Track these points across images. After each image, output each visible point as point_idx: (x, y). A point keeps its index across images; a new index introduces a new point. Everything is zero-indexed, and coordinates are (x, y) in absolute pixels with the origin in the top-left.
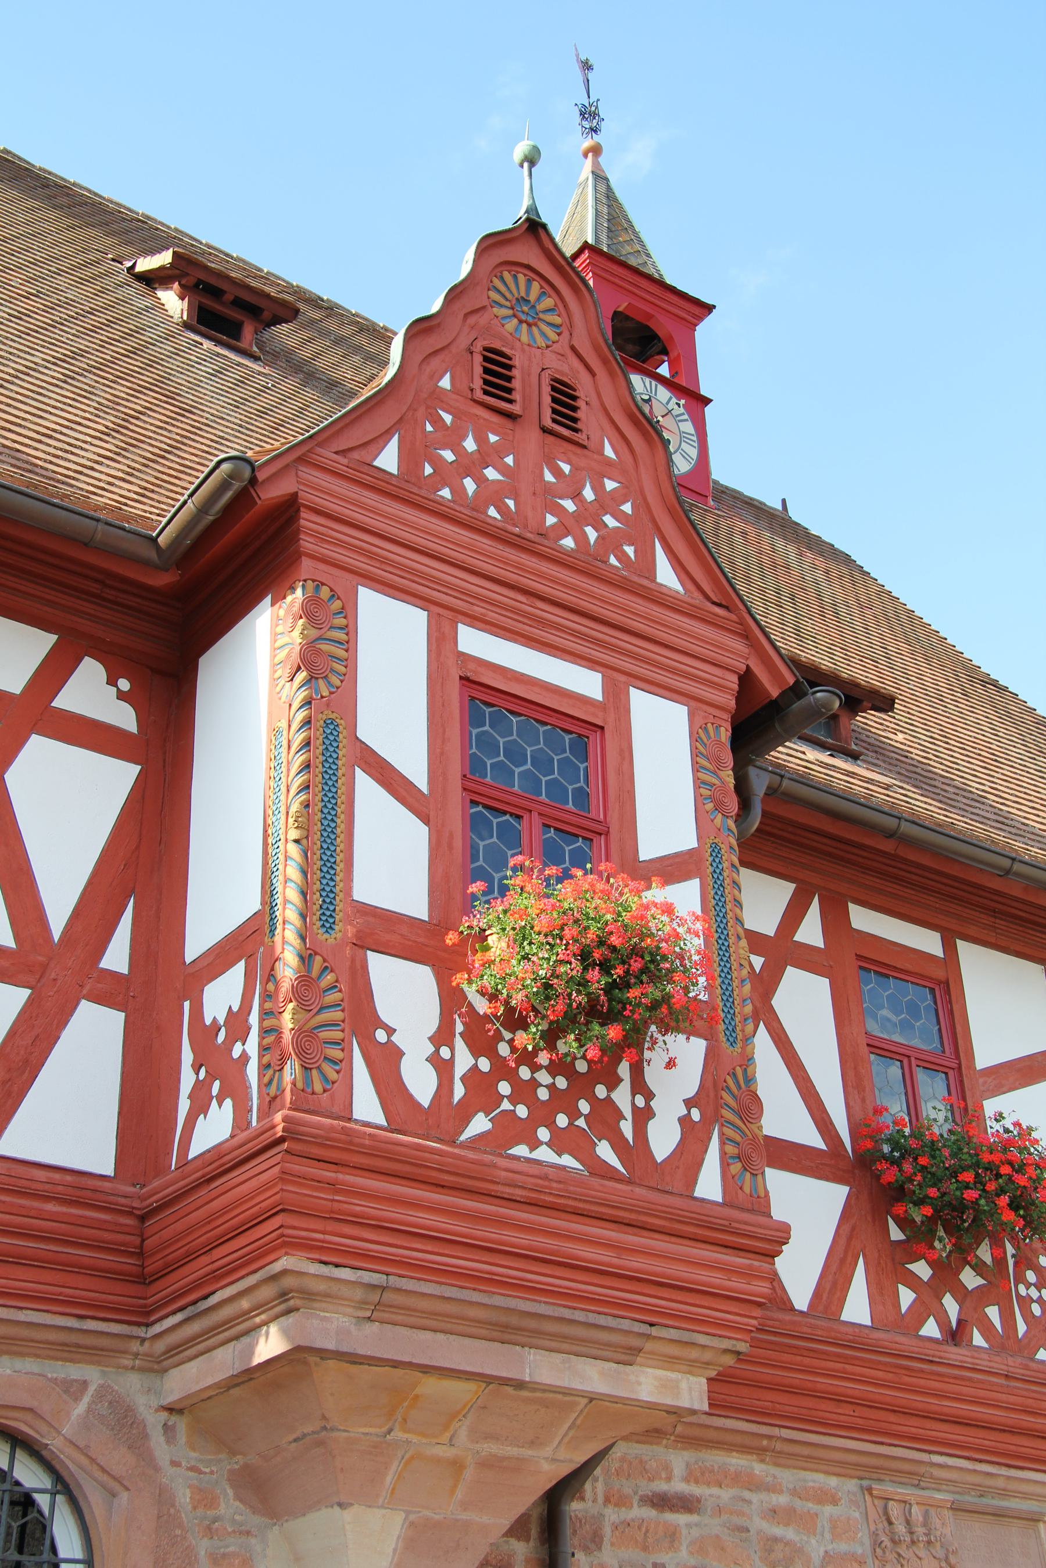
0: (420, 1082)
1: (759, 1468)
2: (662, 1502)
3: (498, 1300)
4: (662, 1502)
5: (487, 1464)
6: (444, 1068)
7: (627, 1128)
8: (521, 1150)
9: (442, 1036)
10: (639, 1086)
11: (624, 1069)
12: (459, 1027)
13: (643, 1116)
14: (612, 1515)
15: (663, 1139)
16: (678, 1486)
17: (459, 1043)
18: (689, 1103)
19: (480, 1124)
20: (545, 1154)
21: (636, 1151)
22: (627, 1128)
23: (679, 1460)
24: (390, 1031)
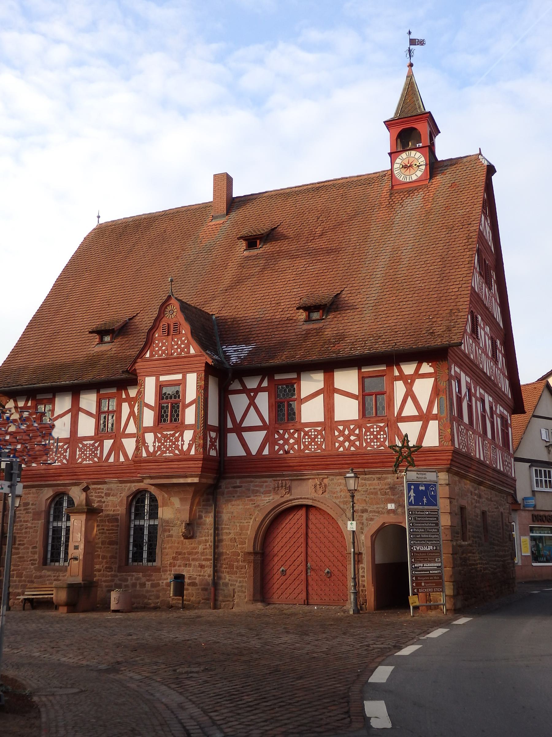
0: (151, 449)
1: (252, 479)
2: (235, 487)
4: (235, 487)
6: (154, 446)
8: (164, 455)
9: (154, 442)
10: (183, 440)
11: (180, 439)
13: (182, 445)
14: (226, 490)
15: (185, 448)
16: (238, 484)
19: (159, 452)
20: (168, 454)
21: (181, 451)
22: (180, 447)
23: (238, 481)
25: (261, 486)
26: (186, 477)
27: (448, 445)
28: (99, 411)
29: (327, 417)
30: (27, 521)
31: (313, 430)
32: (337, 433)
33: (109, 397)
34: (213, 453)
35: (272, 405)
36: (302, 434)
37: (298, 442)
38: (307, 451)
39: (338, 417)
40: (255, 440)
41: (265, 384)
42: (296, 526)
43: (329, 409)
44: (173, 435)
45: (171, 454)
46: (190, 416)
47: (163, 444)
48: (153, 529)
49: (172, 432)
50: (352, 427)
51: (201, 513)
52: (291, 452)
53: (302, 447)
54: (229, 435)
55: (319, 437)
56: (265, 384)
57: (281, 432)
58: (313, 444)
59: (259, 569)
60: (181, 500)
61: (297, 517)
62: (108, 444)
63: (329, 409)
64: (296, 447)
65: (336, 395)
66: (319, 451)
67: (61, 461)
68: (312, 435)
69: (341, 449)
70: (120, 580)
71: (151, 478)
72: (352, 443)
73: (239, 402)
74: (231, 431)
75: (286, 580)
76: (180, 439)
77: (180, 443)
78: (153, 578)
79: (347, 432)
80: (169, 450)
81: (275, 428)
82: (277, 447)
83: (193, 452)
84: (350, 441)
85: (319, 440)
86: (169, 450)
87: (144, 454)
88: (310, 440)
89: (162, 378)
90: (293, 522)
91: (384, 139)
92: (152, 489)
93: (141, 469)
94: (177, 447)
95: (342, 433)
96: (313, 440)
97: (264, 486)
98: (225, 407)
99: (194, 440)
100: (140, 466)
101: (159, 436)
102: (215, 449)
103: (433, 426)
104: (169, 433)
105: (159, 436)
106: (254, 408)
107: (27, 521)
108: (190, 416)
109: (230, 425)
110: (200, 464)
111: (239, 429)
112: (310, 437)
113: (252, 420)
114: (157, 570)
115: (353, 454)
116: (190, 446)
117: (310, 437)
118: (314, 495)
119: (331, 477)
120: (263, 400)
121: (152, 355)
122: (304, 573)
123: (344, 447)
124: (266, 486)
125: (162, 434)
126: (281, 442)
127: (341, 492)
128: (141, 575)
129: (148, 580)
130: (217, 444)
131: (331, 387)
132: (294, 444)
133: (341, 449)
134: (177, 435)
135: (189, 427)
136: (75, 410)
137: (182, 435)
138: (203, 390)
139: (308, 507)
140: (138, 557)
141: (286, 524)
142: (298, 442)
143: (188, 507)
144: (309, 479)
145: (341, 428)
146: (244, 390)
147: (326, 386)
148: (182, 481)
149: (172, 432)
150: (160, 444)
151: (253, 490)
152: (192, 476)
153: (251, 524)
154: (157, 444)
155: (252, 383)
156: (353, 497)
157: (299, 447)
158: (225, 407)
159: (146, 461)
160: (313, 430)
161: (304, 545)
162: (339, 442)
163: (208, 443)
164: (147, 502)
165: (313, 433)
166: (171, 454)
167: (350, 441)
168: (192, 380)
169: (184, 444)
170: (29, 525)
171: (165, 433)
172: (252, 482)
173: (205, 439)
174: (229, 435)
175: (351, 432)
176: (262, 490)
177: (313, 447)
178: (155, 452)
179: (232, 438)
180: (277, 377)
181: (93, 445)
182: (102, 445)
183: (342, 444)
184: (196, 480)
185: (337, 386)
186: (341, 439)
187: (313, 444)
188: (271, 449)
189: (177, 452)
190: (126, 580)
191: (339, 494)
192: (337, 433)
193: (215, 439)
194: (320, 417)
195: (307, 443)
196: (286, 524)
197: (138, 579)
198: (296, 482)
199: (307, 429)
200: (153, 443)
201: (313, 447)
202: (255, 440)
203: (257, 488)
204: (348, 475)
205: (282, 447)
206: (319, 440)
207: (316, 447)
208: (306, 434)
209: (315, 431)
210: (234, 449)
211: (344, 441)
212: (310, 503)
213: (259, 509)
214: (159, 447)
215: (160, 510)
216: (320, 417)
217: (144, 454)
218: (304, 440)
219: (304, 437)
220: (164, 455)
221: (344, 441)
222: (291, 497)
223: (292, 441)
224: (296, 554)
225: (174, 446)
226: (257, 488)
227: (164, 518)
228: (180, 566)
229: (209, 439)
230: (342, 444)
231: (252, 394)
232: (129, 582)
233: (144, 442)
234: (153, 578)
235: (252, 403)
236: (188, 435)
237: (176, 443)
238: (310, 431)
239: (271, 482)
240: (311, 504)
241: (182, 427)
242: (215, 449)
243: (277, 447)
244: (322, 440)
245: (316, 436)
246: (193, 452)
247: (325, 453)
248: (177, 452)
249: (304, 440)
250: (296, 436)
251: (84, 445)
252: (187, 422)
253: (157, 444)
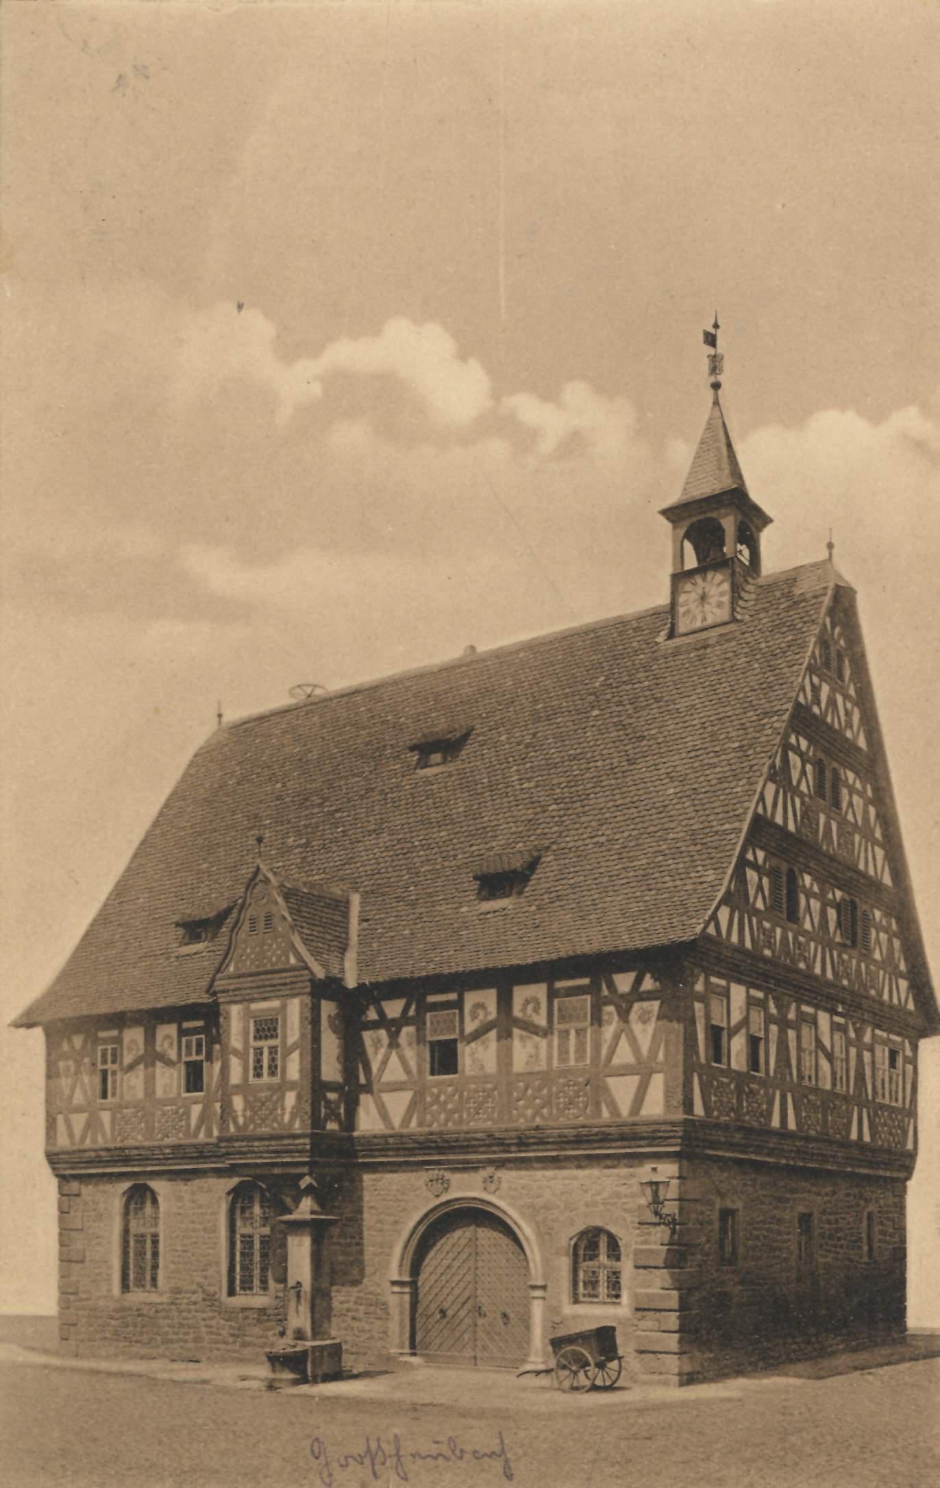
0: (241, 1121)
6: (244, 1116)
9: (245, 1110)
10: (283, 1109)
13: (283, 1114)
21: (281, 1123)
27: (680, 1116)
34: (332, 1126)
41: (412, 1012)
91: (663, 549)
94: (275, 1120)
103: (658, 1081)
116: (293, 1116)
121: (237, 968)
134: (275, 1098)
168: (295, 1010)
178: (246, 1125)
189: (275, 1125)
202: (397, 1104)
210: (368, 1122)
246: (297, 1125)
248: (275, 1125)
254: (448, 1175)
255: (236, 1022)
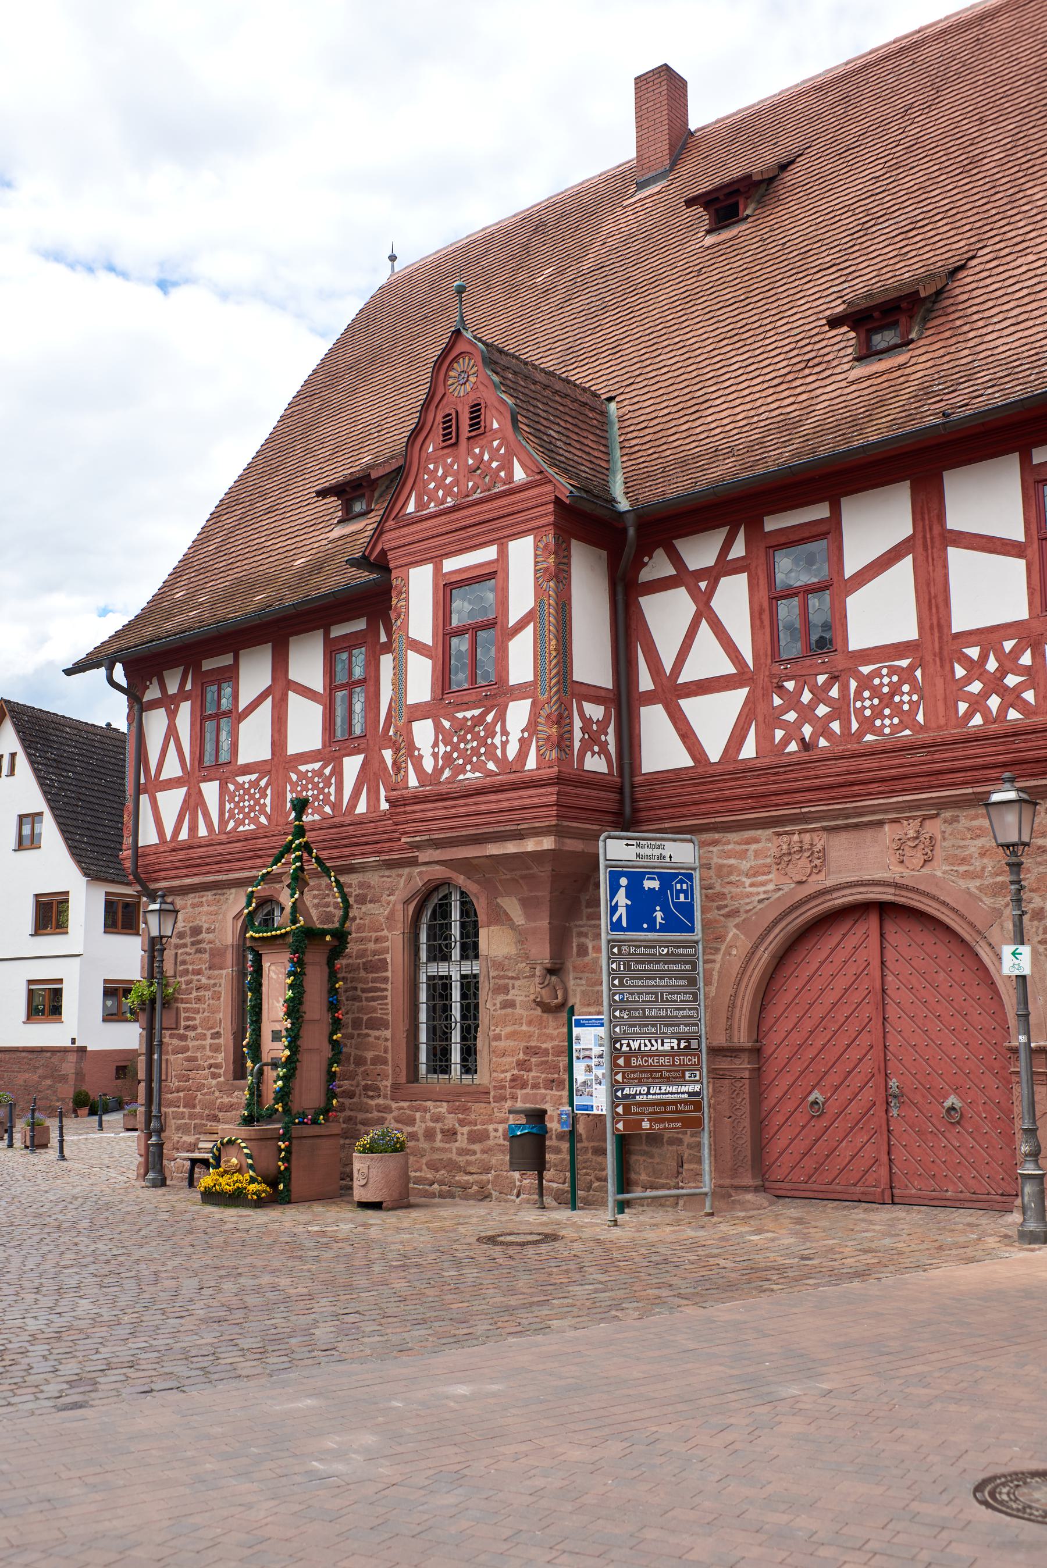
0: (428, 765)
1: (717, 836)
3: (464, 833)
5: (523, 877)
6: (435, 755)
7: (499, 752)
8: (461, 777)
9: (435, 745)
10: (505, 732)
11: (498, 728)
12: (441, 737)
13: (504, 744)
15: (512, 751)
17: (441, 744)
18: (523, 731)
19: (447, 773)
20: (469, 775)
21: (503, 762)
22: (499, 752)
24: (419, 750)
25: (742, 855)
26: (519, 836)
28: (331, 686)
29: (927, 626)
30: (198, 972)
31: (885, 671)
32: (960, 672)
33: (350, 643)
34: (595, 764)
35: (761, 612)
36: (853, 684)
37: (840, 711)
38: (869, 737)
39: (960, 623)
40: (715, 719)
42: (852, 970)
43: (933, 598)
44: (479, 720)
45: (477, 774)
46: (521, 661)
47: (456, 747)
48: (470, 985)
49: (477, 712)
50: (1008, 645)
51: (583, 940)
52: (823, 743)
53: (855, 726)
54: (644, 710)
55: (906, 688)
56: (738, 550)
57: (790, 685)
58: (887, 712)
59: (747, 1096)
60: (526, 903)
61: (852, 941)
62: (352, 765)
63: (933, 598)
64: (835, 726)
65: (951, 551)
66: (907, 732)
67: (255, 820)
68: (882, 685)
69: (977, 720)
70: (397, 1120)
71: (437, 844)
72: (1011, 697)
73: (667, 615)
74: (650, 698)
75: (827, 1128)
76: (498, 728)
77: (497, 741)
78: (473, 1116)
79: (992, 665)
80: (470, 762)
81: (772, 676)
82: (779, 734)
83: (531, 763)
84: (1002, 691)
85: (906, 698)
86: (470, 762)
87: (413, 781)
88: (876, 701)
89: (450, 565)
90: (841, 956)
92: (461, 880)
93: (407, 822)
94: (491, 755)
95: (976, 669)
96: (887, 700)
97: (751, 854)
98: (627, 632)
99: (532, 726)
100: (405, 813)
101: (447, 724)
102: (604, 751)
104: (469, 714)
105: (447, 724)
106: (706, 625)
107: (198, 972)
108: (521, 661)
109: (646, 682)
110: (549, 795)
111: (671, 693)
112: (876, 692)
113: (708, 660)
114: (481, 1094)
115: (1017, 732)
116: (524, 743)
117: (876, 692)
118: (895, 872)
119: (947, 814)
120: (733, 598)
121: (420, 505)
122: (880, 1108)
123: (986, 712)
124: (757, 854)
125: (452, 719)
126: (791, 716)
127: (982, 855)
128: (443, 1108)
129: (462, 1123)
130: (611, 738)
131: (936, 530)
132: (829, 718)
133: (977, 720)
134: (489, 718)
135: (521, 691)
136: (281, 687)
137: (501, 717)
138: (556, 578)
139: (885, 910)
140: (440, 1062)
141: (822, 963)
142: (840, 711)
143: (544, 923)
144: (880, 823)
145: (974, 652)
146: (683, 577)
147: (920, 528)
148: (511, 848)
149: (477, 712)
150: (449, 749)
151: (720, 867)
152: (536, 833)
153: (717, 966)
154: (442, 749)
155: (700, 553)
156: (1016, 867)
157: (846, 725)
158: (627, 632)
159: (419, 799)
160: (885, 671)
161: (877, 1023)
162: (969, 698)
163: (578, 735)
164: (455, 915)
165: (886, 680)
166: (477, 774)
167: (1002, 691)
168: (523, 555)
169: (507, 741)
170: (204, 980)
171: (460, 715)
172: (715, 843)
173: (562, 720)
174: (644, 710)
175: (1008, 665)
176: (745, 865)
177: (887, 722)
178: (438, 771)
179: (653, 719)
180: (772, 524)
181: (319, 773)
182: (338, 772)
183: (977, 703)
184: (547, 843)
185: (950, 526)
186: (976, 687)
187: (887, 712)
188: (764, 739)
189: (491, 766)
190: (412, 1122)
191: (978, 864)
192: (960, 672)
193: (603, 724)
194: (906, 628)
195: (868, 712)
196: (822, 963)
197: (437, 1119)
198: (843, 838)
199: (866, 670)
200: (433, 747)
201: (887, 723)
202: (715, 719)
203: (732, 861)
204: (996, 797)
205: (793, 731)
206: (905, 698)
207: (896, 721)
208: (865, 683)
209: (893, 671)
210: (661, 750)
211: (985, 695)
212: (887, 895)
213: (737, 920)
214: (448, 756)
215: (483, 932)
216: (906, 628)
217: (413, 781)
218: (859, 704)
219: (858, 695)
220: (461, 777)
221: (985, 695)
222: (829, 883)
223: (822, 710)
224: (854, 1054)
225: (483, 750)
226: (732, 861)
227: (492, 954)
228: (535, 1086)
229: (578, 723)
230: (977, 703)
231: (703, 585)
232: (419, 1128)
233: (411, 746)
234: (473, 1116)
235: (705, 612)
236: (518, 714)
237: (489, 741)
238: (877, 673)
239: (769, 840)
240: (890, 898)
241: (497, 694)
242: (604, 751)
243: (779, 734)
244: (915, 697)
245: (896, 689)
246: (531, 763)
247: (926, 737)
248: (491, 766)
249: (859, 704)
250: (834, 692)
251: (302, 776)
252: (514, 679)
253: (442, 749)
254: (820, 841)
255: (419, 587)
